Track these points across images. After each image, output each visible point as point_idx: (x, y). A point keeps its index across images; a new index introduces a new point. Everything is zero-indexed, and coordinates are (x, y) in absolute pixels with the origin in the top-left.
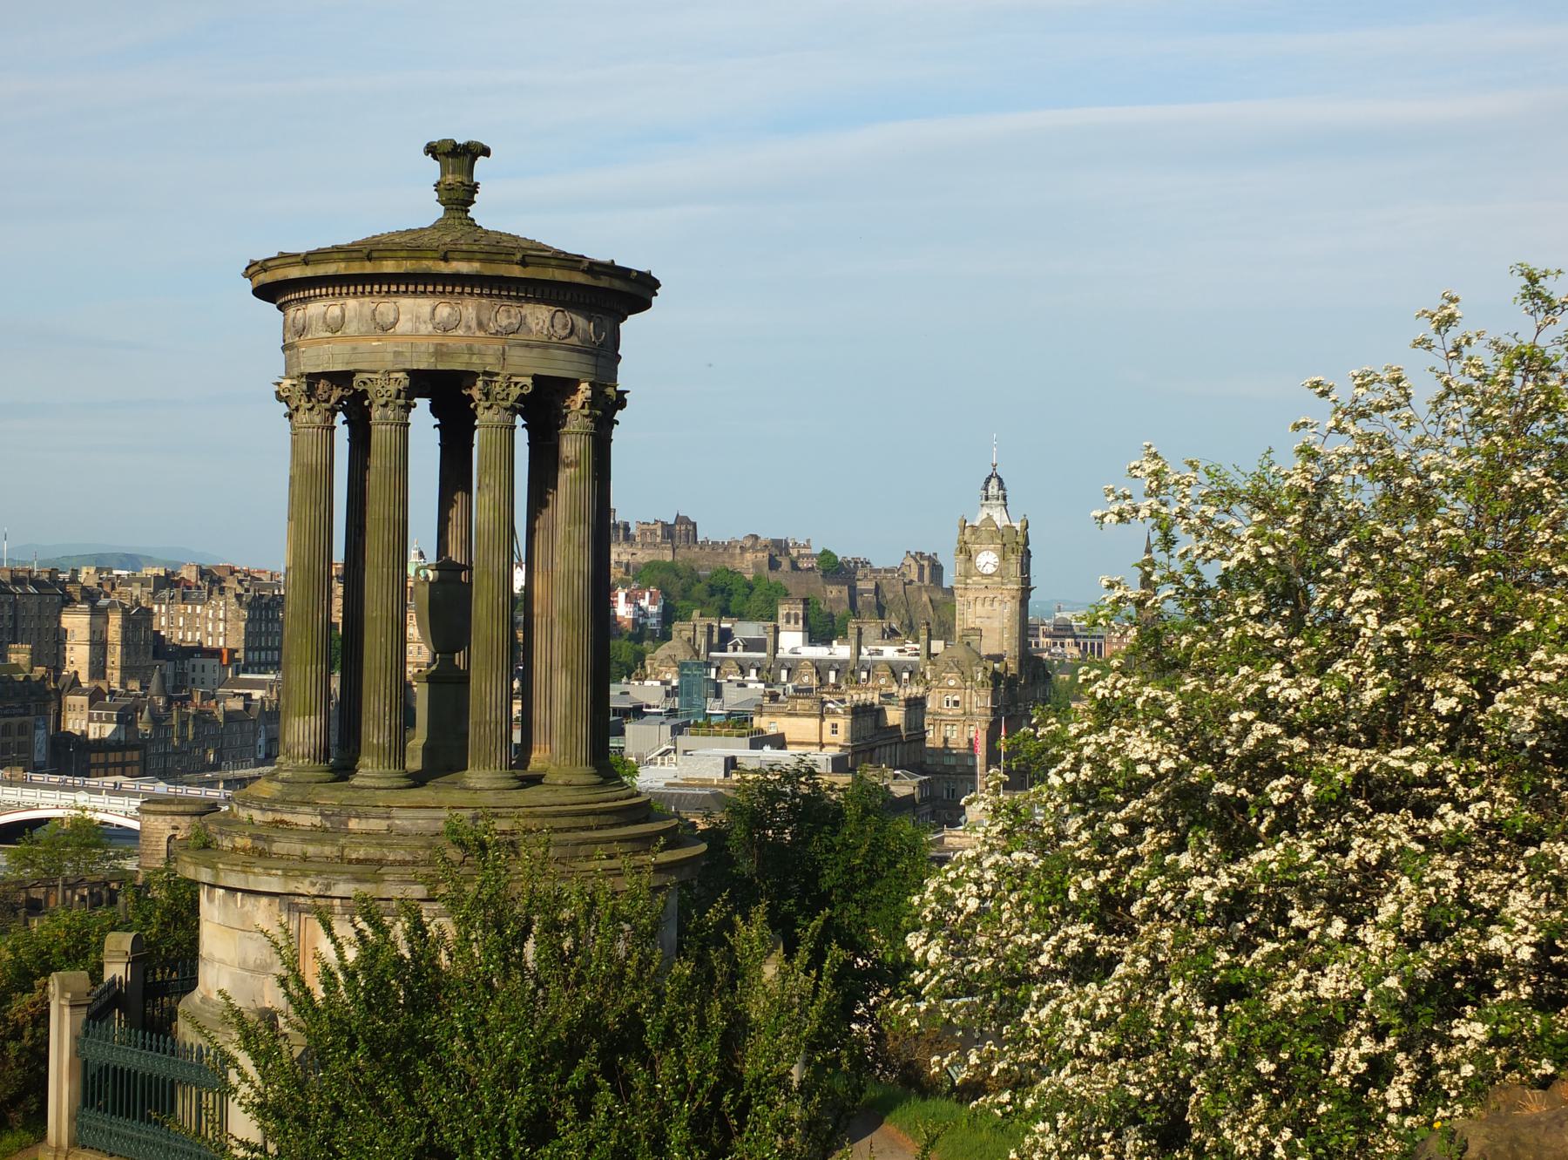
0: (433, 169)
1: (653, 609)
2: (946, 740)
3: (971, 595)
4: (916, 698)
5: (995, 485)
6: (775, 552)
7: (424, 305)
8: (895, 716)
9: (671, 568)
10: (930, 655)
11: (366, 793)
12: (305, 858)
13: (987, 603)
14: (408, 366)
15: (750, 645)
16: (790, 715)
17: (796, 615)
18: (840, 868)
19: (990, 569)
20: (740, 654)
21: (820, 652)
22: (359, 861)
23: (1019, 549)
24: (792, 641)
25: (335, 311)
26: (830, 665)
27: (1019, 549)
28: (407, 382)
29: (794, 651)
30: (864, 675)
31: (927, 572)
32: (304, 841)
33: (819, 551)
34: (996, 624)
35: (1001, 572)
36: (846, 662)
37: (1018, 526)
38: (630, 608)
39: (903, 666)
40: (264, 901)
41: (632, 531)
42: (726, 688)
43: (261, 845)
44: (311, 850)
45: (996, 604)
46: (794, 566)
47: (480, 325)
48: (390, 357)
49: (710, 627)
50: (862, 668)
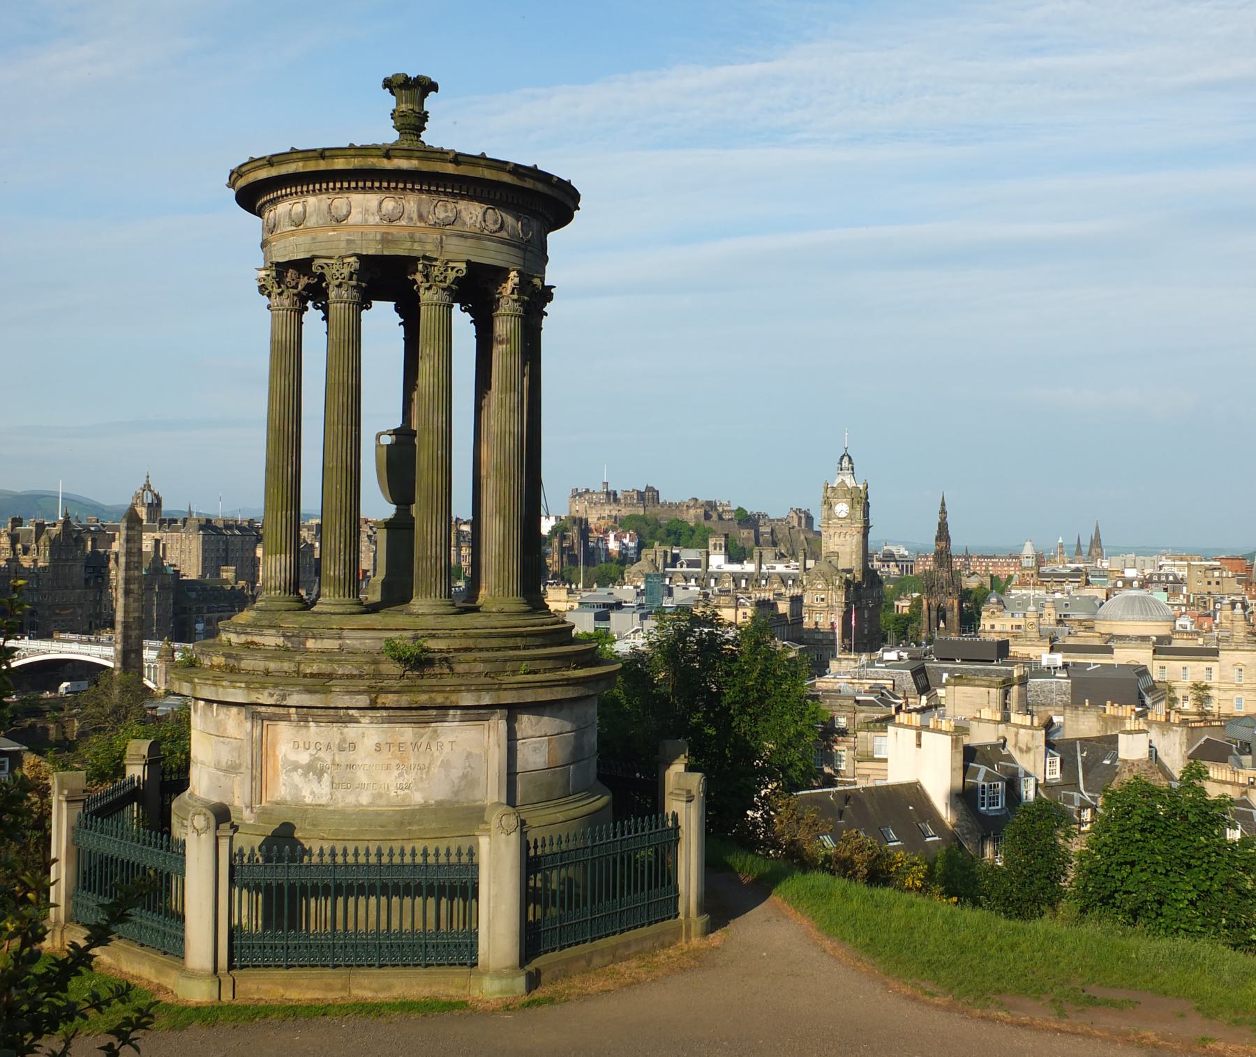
0: (389, 102)
1: (632, 545)
2: (816, 623)
3: (832, 531)
5: (847, 461)
7: (372, 199)
8: (783, 607)
9: (643, 519)
10: (805, 569)
11: (323, 618)
12: (267, 673)
14: (358, 252)
15: (691, 564)
18: (737, 689)
19: (843, 515)
20: (685, 569)
21: (736, 568)
22: (312, 675)
23: (862, 501)
24: (717, 561)
25: (299, 208)
27: (862, 501)
28: (357, 265)
29: (719, 567)
30: (763, 582)
31: (803, 521)
32: (266, 658)
34: (848, 550)
35: (850, 516)
36: (752, 574)
38: (617, 544)
39: (789, 576)
40: (234, 710)
42: (675, 591)
43: (232, 662)
44: (272, 666)
47: (421, 217)
48: (343, 245)
49: (665, 552)
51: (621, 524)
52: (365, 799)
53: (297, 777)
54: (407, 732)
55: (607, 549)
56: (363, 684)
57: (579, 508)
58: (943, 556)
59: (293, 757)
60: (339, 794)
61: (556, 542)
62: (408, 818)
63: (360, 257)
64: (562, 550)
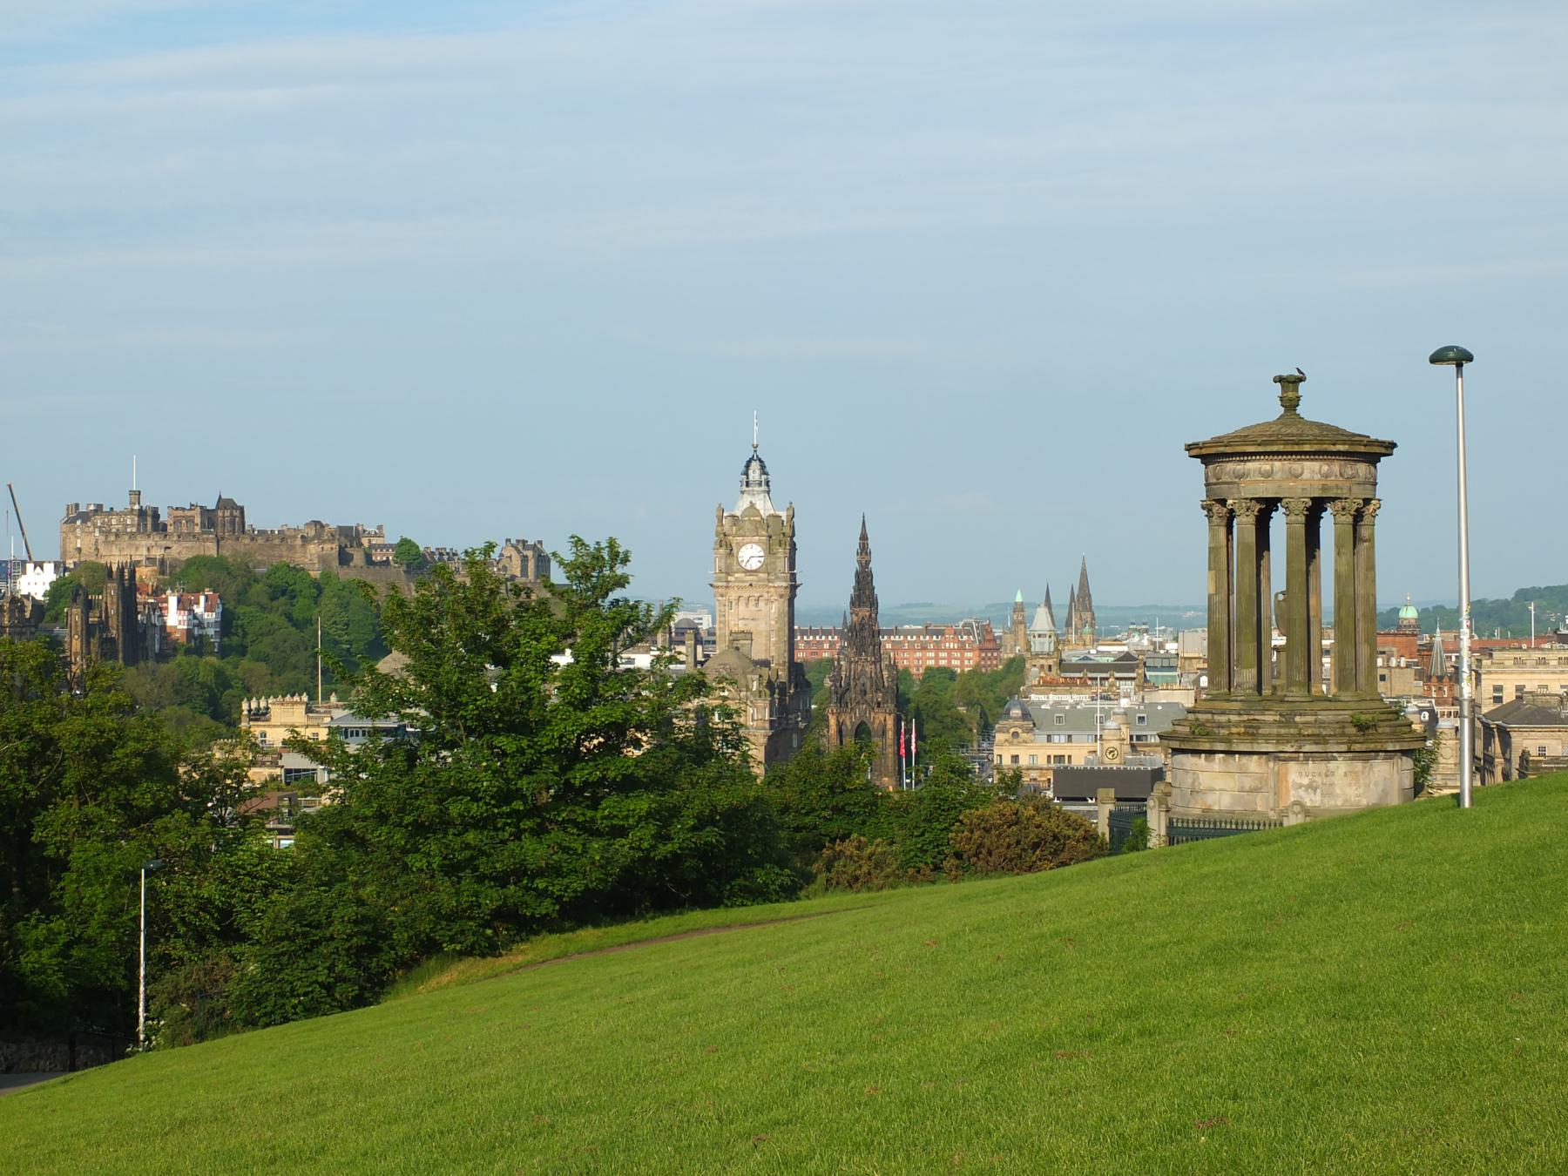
1: (210, 617)
3: (733, 595)
6: (344, 541)
7: (1315, 465)
9: (219, 564)
12: (1279, 735)
13: (752, 602)
23: (783, 539)
25: (1268, 467)
27: (783, 539)
31: (531, 565)
33: (396, 541)
34: (762, 627)
35: (767, 568)
37: (784, 515)
38: (184, 616)
40: (1255, 757)
41: (164, 518)
44: (1283, 731)
45: (762, 604)
46: (369, 560)
51: (186, 577)
52: (1339, 803)
53: (1301, 792)
54: (1359, 765)
55: (164, 627)
56: (1345, 739)
57: (84, 542)
61: (76, 615)
64: (89, 631)
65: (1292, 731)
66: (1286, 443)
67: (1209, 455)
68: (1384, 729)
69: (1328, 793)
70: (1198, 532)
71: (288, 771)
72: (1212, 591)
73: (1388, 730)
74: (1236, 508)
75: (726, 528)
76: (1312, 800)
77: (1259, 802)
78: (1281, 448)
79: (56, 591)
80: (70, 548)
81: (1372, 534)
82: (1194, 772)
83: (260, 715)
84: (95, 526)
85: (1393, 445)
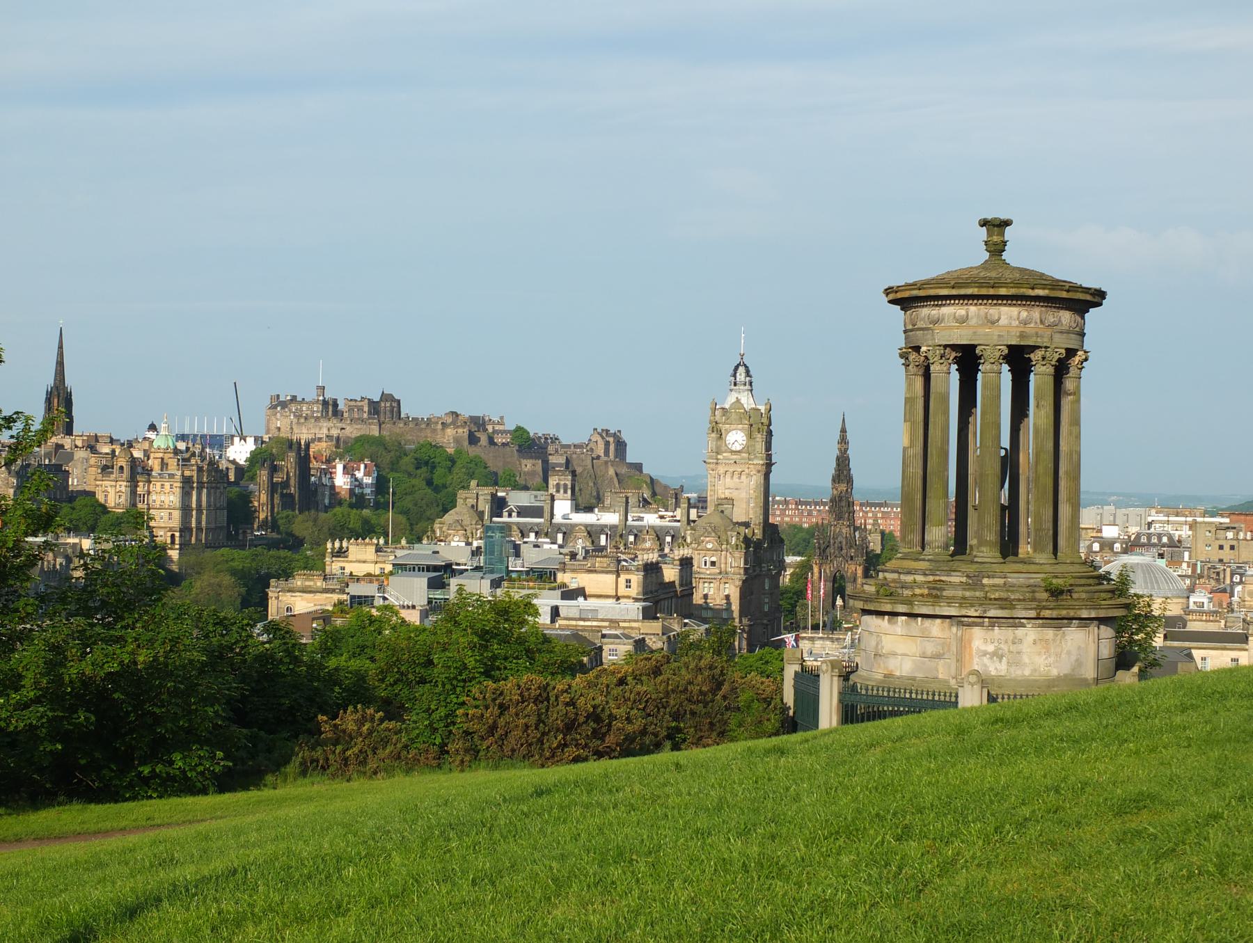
1: (368, 480)
2: (706, 597)
3: (721, 469)
4: (687, 558)
5: (742, 372)
7: (1014, 311)
8: (670, 574)
9: (379, 442)
10: (689, 521)
12: (964, 598)
13: (736, 476)
15: (523, 512)
16: (590, 571)
17: (565, 485)
19: (737, 447)
20: (515, 519)
23: (762, 428)
24: (563, 507)
26: (602, 529)
27: (762, 428)
29: (565, 517)
30: (631, 538)
31: (612, 447)
33: (513, 428)
34: (744, 495)
35: (748, 449)
36: (613, 528)
37: (762, 408)
38: (348, 479)
40: (938, 621)
41: (341, 407)
42: (524, 548)
44: (968, 594)
45: (743, 477)
50: (630, 532)
51: (349, 450)
52: (1027, 673)
53: (986, 660)
54: (1050, 633)
55: (333, 487)
56: (1034, 604)
57: (283, 424)
58: (842, 505)
59: (983, 648)
60: (1012, 670)
61: (263, 475)
62: (1052, 683)
63: (1009, 347)
64: (273, 488)
65: (978, 594)
66: (981, 286)
67: (905, 300)
68: (1080, 594)
69: (1015, 662)
70: (896, 384)
71: (353, 597)
72: (906, 443)
73: (1084, 596)
74: (930, 355)
75: (718, 418)
76: (996, 669)
77: (941, 670)
78: (975, 291)
79: (254, 458)
80: (273, 427)
81: (1078, 387)
82: (878, 635)
83: (341, 553)
84: (290, 411)
85: (1101, 294)
